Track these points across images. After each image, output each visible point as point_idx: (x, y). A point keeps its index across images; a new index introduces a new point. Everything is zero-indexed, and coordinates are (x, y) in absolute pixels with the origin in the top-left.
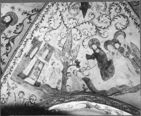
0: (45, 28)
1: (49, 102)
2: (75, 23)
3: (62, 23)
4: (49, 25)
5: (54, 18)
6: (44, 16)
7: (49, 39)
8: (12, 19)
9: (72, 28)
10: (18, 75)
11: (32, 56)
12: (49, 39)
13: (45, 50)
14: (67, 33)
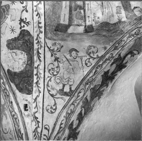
1: (117, 45)
10: (55, 30)
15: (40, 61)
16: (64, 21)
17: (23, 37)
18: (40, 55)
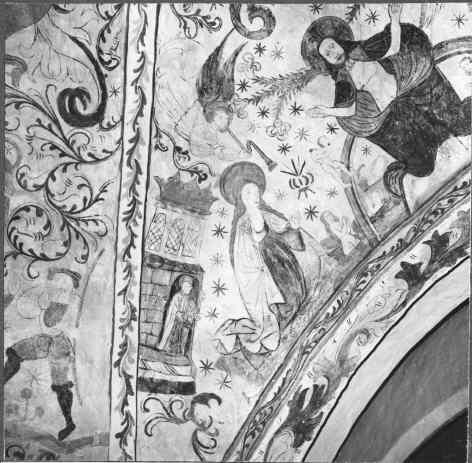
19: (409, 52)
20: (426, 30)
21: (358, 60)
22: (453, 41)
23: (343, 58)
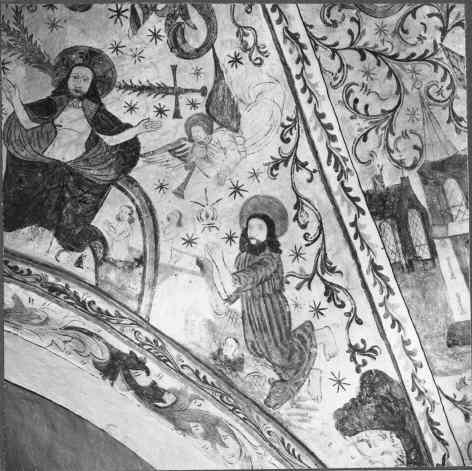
0: (365, 137)
2: (430, 16)
3: (396, 66)
4: (368, 115)
5: (353, 84)
6: (320, 116)
7: (415, 147)
8: (264, 218)
9: (439, 41)
10: (449, 346)
11: (426, 249)
12: (415, 147)
13: (443, 191)
14: (446, 70)
15: (445, 444)
16: (463, 312)
17: (373, 390)
18: (438, 427)
19: (114, 156)
20: (140, 162)
21: (84, 110)
22: (141, 190)
23: (79, 94)
